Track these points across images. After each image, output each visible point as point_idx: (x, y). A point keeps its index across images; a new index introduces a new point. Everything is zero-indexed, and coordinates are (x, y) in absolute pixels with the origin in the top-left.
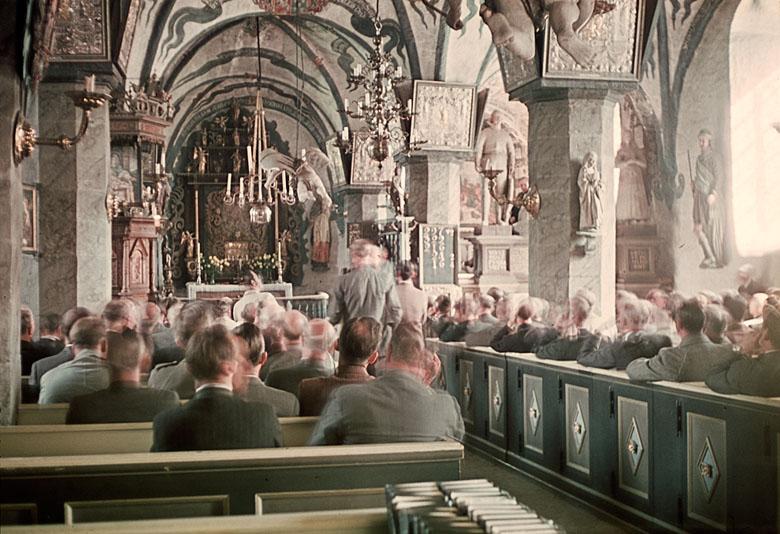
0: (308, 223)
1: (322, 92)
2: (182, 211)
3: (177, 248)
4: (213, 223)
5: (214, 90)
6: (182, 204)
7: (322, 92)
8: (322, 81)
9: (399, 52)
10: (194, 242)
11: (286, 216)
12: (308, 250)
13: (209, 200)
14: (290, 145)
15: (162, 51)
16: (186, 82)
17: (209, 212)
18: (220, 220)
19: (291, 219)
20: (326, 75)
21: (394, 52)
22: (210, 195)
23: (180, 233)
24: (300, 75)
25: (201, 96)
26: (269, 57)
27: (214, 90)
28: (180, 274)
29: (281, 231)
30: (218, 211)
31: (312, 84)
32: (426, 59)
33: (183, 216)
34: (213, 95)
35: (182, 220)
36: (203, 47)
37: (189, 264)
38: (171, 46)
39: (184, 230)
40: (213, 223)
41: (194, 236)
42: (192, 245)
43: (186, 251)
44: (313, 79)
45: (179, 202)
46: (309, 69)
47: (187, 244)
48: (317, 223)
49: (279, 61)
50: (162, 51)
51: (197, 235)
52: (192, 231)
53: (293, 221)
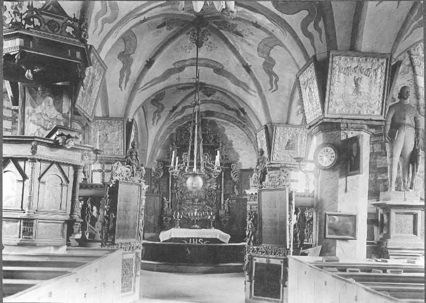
1: (251, 95)
5: (183, 105)
7: (251, 95)
8: (252, 86)
9: (316, 26)
10: (168, 204)
14: (233, 143)
15: (97, 25)
16: (151, 86)
20: (254, 79)
21: (311, 28)
24: (238, 83)
25: (175, 108)
26: (212, 67)
27: (183, 105)
29: (225, 199)
31: (244, 89)
32: (342, 35)
34: (184, 109)
36: (161, 55)
37: (164, 219)
38: (105, 21)
41: (168, 201)
44: (245, 84)
46: (243, 76)
49: (220, 70)
50: (97, 25)
51: (170, 200)
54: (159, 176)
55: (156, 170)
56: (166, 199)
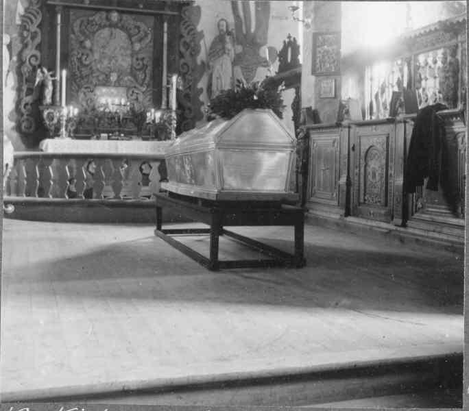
0: (205, 66)
2: (38, 40)
3: (30, 91)
4: (79, 60)
6: (38, 30)
11: (177, 58)
12: (202, 104)
13: (76, 29)
17: (74, 44)
18: (91, 56)
19: (182, 61)
22: (78, 22)
23: (34, 70)
28: (33, 129)
30: (88, 44)
33: (39, 47)
35: (38, 54)
37: (46, 113)
39: (40, 66)
40: (79, 60)
42: (50, 87)
43: (40, 98)
45: (34, 28)
47: (43, 86)
48: (218, 67)
52: (52, 68)
53: (185, 64)
54: (32, 22)
55: (26, 10)
56: (49, 70)
